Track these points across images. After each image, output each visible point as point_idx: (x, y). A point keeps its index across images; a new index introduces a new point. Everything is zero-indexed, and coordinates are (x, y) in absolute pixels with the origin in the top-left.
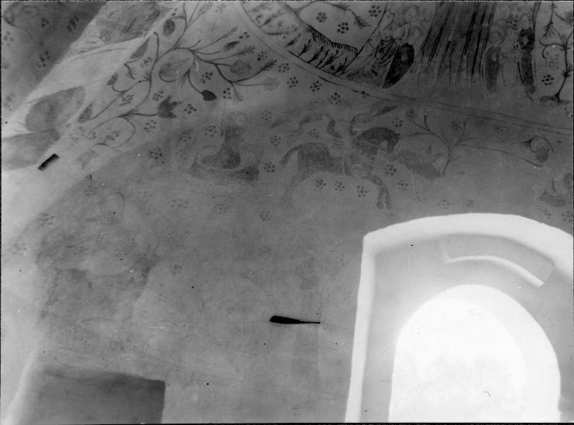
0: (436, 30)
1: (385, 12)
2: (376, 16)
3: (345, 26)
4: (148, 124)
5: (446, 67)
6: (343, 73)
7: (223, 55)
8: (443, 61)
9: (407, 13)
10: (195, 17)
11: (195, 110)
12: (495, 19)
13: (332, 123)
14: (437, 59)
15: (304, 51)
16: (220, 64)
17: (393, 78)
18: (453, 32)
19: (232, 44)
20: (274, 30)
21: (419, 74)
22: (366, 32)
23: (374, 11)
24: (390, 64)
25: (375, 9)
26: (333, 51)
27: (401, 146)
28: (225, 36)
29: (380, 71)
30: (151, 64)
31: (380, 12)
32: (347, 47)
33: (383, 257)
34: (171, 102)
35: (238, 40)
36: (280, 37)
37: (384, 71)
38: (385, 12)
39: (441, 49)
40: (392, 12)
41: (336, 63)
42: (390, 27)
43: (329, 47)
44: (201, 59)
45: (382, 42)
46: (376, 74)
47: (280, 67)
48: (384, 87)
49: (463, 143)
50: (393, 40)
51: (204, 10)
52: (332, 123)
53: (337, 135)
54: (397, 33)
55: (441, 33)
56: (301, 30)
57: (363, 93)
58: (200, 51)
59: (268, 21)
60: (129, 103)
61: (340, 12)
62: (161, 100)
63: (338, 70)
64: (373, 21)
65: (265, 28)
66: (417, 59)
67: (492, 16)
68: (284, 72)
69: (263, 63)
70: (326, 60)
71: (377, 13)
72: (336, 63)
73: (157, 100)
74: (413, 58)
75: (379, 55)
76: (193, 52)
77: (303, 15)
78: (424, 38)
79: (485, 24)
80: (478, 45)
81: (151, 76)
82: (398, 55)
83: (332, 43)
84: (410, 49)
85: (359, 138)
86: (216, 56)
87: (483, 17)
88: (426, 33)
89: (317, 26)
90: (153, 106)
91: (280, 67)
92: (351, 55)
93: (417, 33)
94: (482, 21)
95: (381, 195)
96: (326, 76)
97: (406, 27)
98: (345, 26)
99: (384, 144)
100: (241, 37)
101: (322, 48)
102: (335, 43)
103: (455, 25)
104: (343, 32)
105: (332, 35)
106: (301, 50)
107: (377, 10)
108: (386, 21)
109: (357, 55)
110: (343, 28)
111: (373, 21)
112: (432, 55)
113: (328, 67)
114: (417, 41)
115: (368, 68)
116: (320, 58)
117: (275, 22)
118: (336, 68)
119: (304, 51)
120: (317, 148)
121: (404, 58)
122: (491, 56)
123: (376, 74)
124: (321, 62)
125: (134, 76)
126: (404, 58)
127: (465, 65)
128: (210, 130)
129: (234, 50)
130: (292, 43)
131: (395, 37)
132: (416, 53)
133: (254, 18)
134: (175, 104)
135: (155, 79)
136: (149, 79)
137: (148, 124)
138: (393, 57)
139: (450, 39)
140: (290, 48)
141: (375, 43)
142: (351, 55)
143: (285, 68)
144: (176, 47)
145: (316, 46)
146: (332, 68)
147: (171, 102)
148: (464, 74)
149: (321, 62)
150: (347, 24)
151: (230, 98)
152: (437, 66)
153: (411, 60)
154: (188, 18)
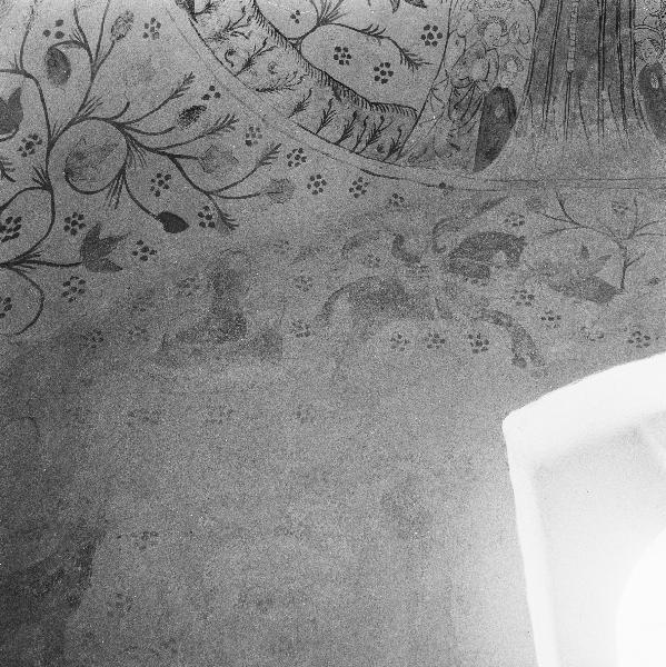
0: (543, 56)
1: (449, 35)
2: (435, 43)
3: (386, 69)
4: (68, 284)
5: (575, 118)
6: (400, 156)
8: (567, 109)
9: (487, 34)
10: (106, 42)
11: (153, 252)
12: (638, 19)
13: (399, 240)
14: (558, 106)
15: (324, 123)
16: (179, 156)
17: (488, 153)
18: (571, 55)
19: (191, 114)
20: (264, 81)
21: (533, 136)
22: (425, 75)
23: (431, 36)
24: (477, 126)
25: (431, 30)
26: (375, 117)
27: (529, 257)
28: (176, 94)
29: (463, 142)
30: (41, 149)
31: (440, 36)
32: (398, 107)
33: (543, 474)
34: (103, 235)
35: (199, 102)
36: (278, 97)
37: (470, 140)
38: (449, 35)
39: (561, 88)
40: (461, 33)
41: (386, 139)
42: (462, 61)
43: (367, 111)
44: (141, 146)
45: (455, 90)
46: (458, 149)
47: (289, 156)
48: (475, 170)
49: (638, 233)
50: (473, 84)
51: (121, 31)
52: (399, 240)
53: (411, 260)
54: (477, 72)
55: (552, 63)
56: (310, 82)
57: (442, 185)
58: (133, 126)
59: (249, 63)
60: (16, 235)
61: (373, 45)
62: (82, 233)
63: (392, 151)
64: (431, 54)
65: (246, 77)
66: (524, 112)
67: (632, 14)
68: (297, 164)
69: (256, 152)
70: (366, 137)
71: (436, 39)
72: (386, 139)
73: (74, 232)
74: (515, 113)
75: (455, 116)
76: (120, 126)
77: (308, 48)
78: (525, 74)
79: (625, 31)
80: (621, 68)
81: (47, 177)
82: (488, 109)
83: (371, 104)
84: (505, 94)
85: (452, 256)
86: (170, 139)
87: (618, 18)
88: (526, 64)
89: (337, 72)
90: (71, 247)
91: (289, 156)
92: (407, 121)
93: (511, 66)
94: (618, 26)
95: (515, 342)
96: (371, 165)
97: (491, 57)
98: (386, 69)
99: (501, 256)
100: (206, 97)
101: (355, 115)
102: (376, 104)
103: (573, 43)
104: (384, 81)
105: (365, 84)
106: (318, 122)
108: (454, 53)
109: (418, 118)
110: (383, 73)
111: (431, 54)
112: (546, 102)
113: (373, 149)
114: (514, 79)
115: (443, 139)
116: (355, 133)
117: (261, 65)
118: (387, 148)
119: (324, 123)
120: (382, 284)
121: (499, 112)
122: (649, 80)
123: (458, 149)
124: (359, 142)
125: (10, 174)
126: (499, 112)
127: (607, 108)
128: (188, 286)
129: (196, 127)
130: (300, 108)
131: (475, 77)
132: (518, 100)
133: (221, 55)
134: (112, 240)
135: (61, 188)
136: (47, 187)
137: (68, 284)
138: (479, 113)
139: (570, 67)
141: (444, 93)
142: (407, 121)
143: (297, 157)
144: (84, 113)
145: (343, 111)
146: (380, 149)
147: (103, 235)
148: (610, 122)
149: (359, 142)
150: (388, 65)
151: (212, 225)
152: (559, 118)
153: (512, 114)
154: (93, 45)
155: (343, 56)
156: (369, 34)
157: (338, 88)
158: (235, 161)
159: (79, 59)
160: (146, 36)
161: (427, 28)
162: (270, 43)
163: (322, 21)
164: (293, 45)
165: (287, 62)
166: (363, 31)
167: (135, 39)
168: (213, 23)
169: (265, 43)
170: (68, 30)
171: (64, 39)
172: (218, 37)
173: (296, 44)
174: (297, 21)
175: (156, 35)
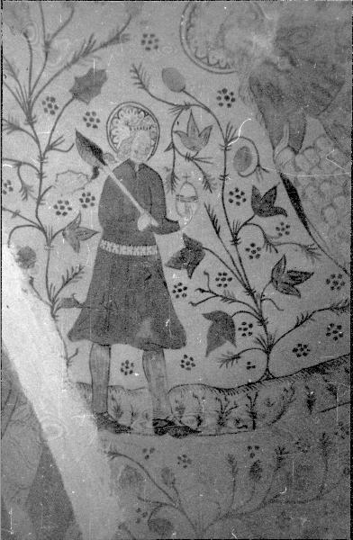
3: (334, 328)
7: (261, 489)
10: (171, 492)
19: (255, 470)
20: (272, 413)
23: (336, 283)
25: (332, 281)
31: (340, 276)
36: (290, 411)
51: (171, 480)
56: (300, 384)
59: (253, 415)
61: (308, 325)
89: (307, 362)
107: (336, 279)
110: (335, 332)
117: (260, 408)
129: (266, 471)
130: (310, 403)
140: (316, 407)
154: (165, 500)
155: (302, 350)
156: (302, 323)
157: (318, 369)
158: (308, 469)
159: (166, 513)
160: (185, 467)
161: (328, 282)
162: (252, 395)
163: (268, 351)
164: (267, 379)
165: (271, 392)
166: (297, 326)
167: (185, 477)
168: (210, 421)
169: (249, 398)
170: (144, 508)
171: (149, 513)
172: (221, 423)
173: (269, 376)
174: (254, 367)
175: (189, 461)
